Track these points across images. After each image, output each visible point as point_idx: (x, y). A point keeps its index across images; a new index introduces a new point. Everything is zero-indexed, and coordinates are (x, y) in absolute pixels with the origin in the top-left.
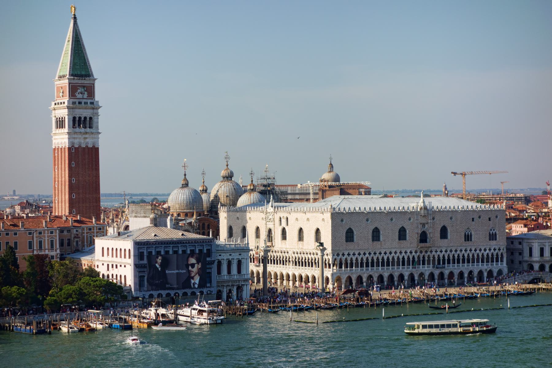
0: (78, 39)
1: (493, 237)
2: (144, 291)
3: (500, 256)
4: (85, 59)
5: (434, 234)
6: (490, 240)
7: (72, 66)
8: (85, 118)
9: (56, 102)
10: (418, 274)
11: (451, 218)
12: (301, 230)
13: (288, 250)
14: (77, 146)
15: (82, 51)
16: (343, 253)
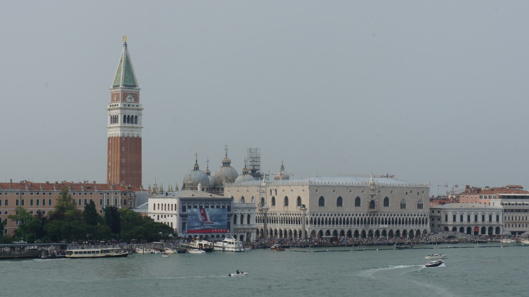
0: (128, 60)
1: (420, 206)
2: (185, 233)
3: (425, 220)
4: (132, 73)
5: (380, 203)
6: (418, 208)
7: (124, 79)
8: (132, 116)
9: (112, 104)
10: (368, 230)
11: (391, 192)
12: (286, 199)
13: (276, 212)
14: (126, 136)
15: (131, 69)
16: (317, 214)
